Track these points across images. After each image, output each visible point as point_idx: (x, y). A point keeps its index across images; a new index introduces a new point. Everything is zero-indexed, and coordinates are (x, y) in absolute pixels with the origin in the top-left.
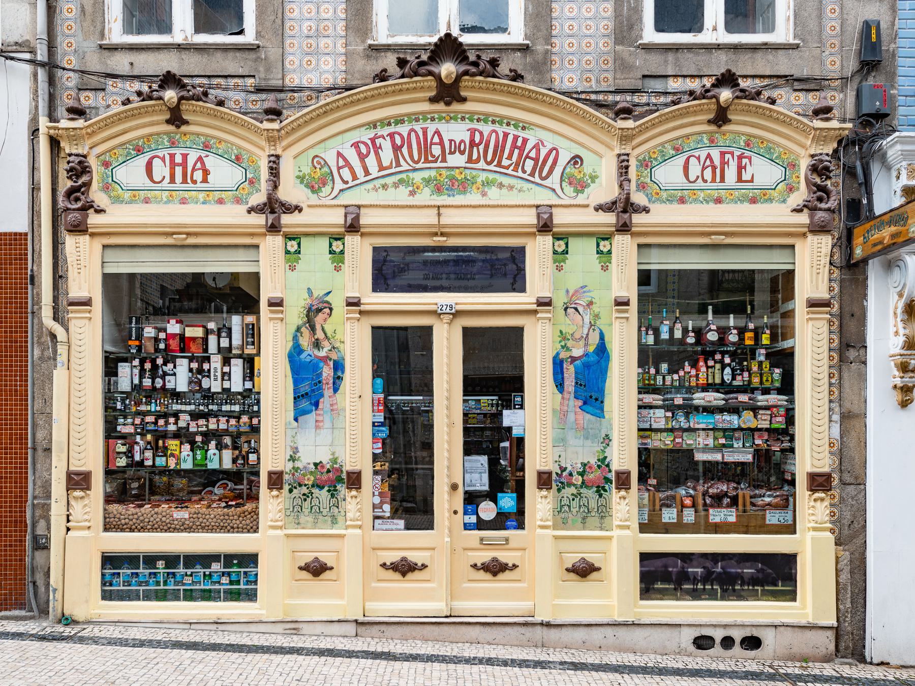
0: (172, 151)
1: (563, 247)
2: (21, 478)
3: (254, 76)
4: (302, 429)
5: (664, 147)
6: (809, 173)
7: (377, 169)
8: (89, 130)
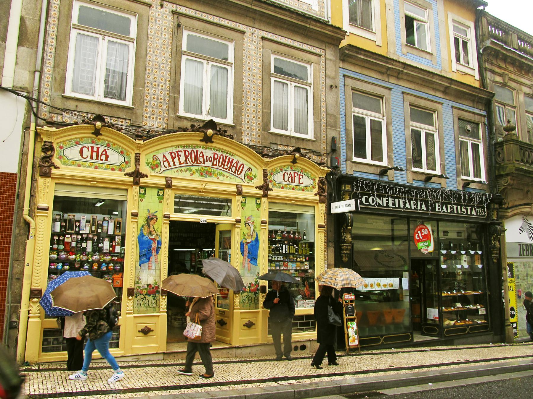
0: (93, 145)
1: (245, 201)
8: (57, 133)
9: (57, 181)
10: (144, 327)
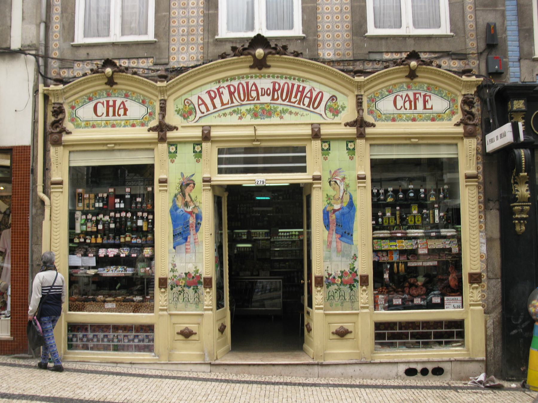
0: (108, 99)
1: (327, 147)
2: (25, 281)
3: (153, 57)
4: (178, 253)
5: (382, 90)
6: (462, 105)
7: (220, 105)
9: (72, 149)
10: (339, 327)
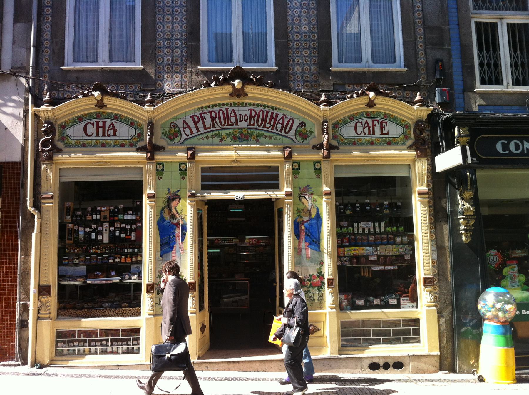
1: (297, 167)
2: (13, 290)
4: (164, 261)
7: (203, 129)
